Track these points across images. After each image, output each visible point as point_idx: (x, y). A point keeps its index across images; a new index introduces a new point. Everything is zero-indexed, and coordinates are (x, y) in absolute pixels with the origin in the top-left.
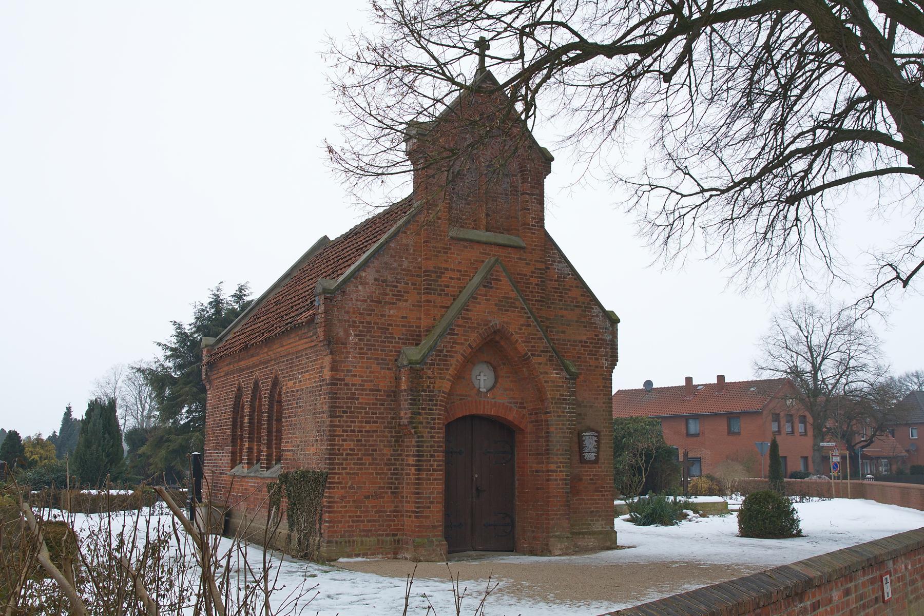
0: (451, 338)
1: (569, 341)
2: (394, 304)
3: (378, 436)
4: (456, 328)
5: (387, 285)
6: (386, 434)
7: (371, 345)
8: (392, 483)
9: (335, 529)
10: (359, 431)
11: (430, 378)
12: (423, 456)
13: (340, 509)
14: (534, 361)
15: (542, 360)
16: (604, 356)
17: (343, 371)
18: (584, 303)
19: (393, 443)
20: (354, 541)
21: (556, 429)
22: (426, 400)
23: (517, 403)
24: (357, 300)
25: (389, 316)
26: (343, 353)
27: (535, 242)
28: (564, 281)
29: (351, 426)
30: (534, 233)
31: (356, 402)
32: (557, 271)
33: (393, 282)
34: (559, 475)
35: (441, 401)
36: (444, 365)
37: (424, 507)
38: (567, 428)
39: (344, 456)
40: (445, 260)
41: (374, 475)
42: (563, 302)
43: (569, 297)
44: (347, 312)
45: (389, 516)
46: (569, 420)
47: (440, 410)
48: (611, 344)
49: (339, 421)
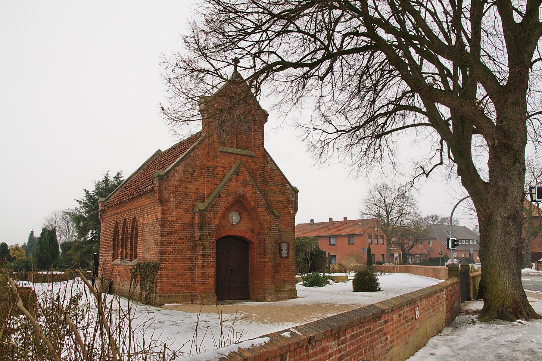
1: (275, 201)
2: (192, 182)
4: (222, 194)
8: (190, 268)
10: (175, 243)
11: (209, 218)
12: (205, 255)
14: (258, 210)
15: (262, 209)
16: (292, 208)
17: (167, 214)
20: (172, 296)
24: (174, 180)
29: (171, 241)
30: (259, 150)
33: (192, 172)
36: (216, 212)
37: (205, 279)
44: (170, 186)
46: (275, 238)
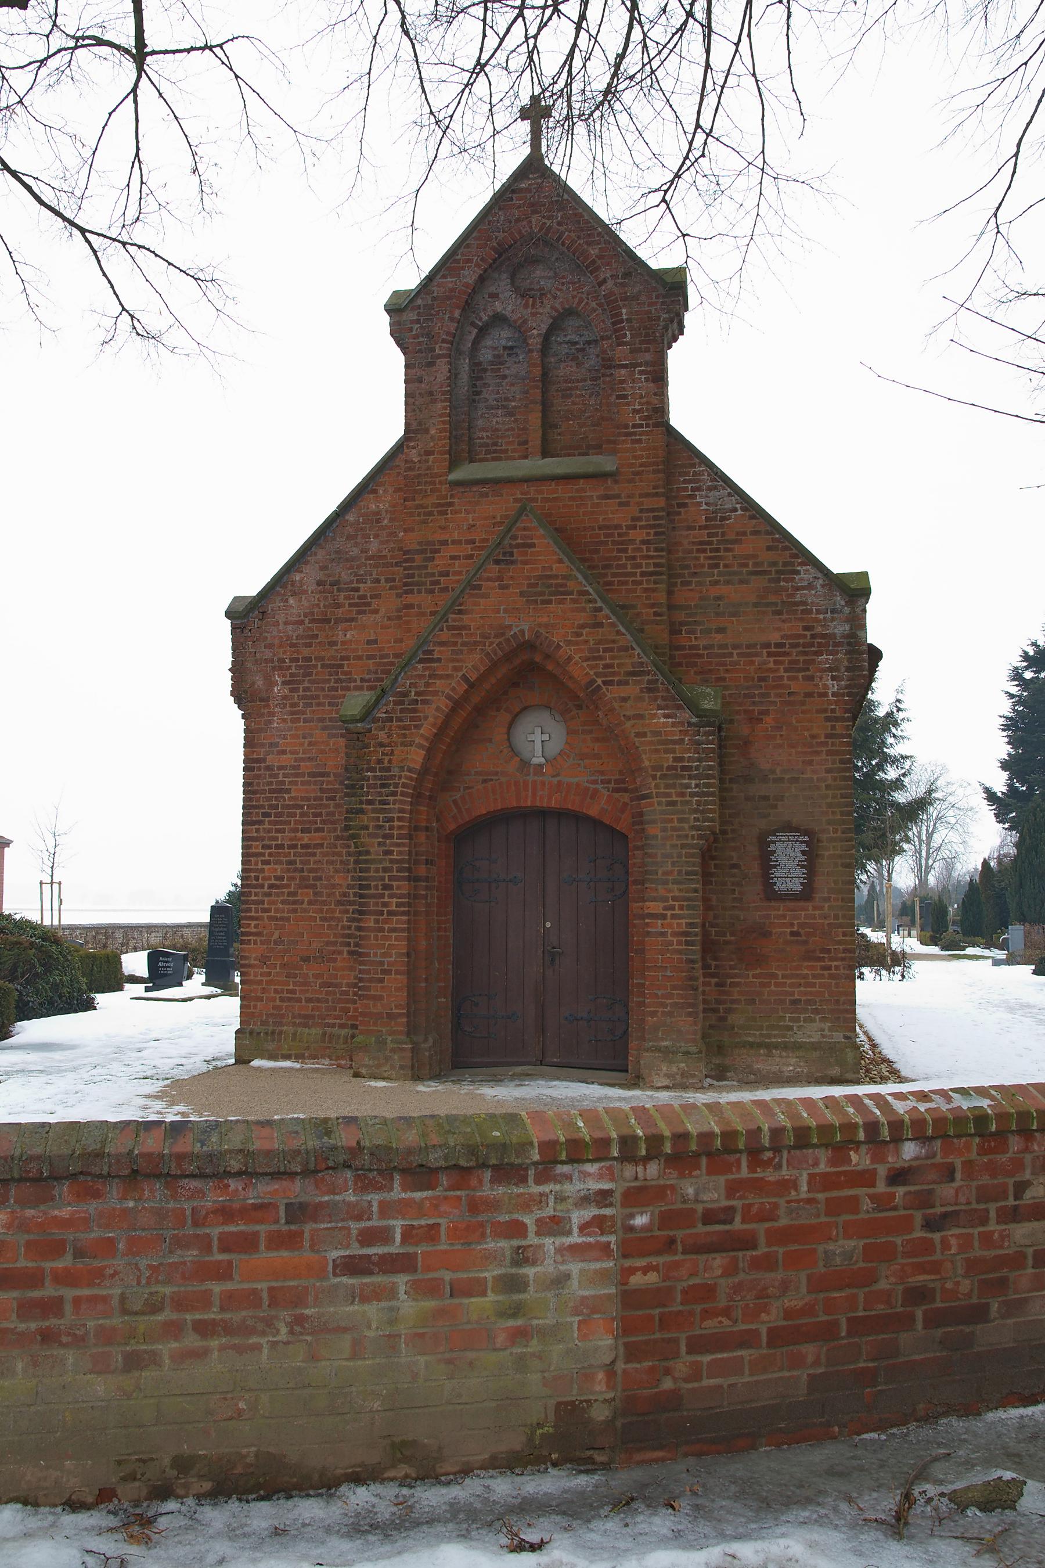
0: (425, 669)
1: (735, 647)
2: (352, 620)
3: (324, 855)
4: (437, 649)
5: (339, 590)
6: (339, 849)
7: (312, 697)
8: (349, 936)
9: (252, 1010)
10: (291, 847)
11: (381, 745)
12: (368, 887)
13: (259, 978)
14: (609, 695)
15: (631, 690)
16: (830, 669)
17: (263, 745)
18: (774, 564)
19: (351, 866)
20: (281, 1033)
21: (664, 830)
22: (375, 786)
23: (609, 782)
24: (286, 623)
25: (343, 643)
26: (263, 715)
27: (642, 457)
28: (722, 526)
29: (276, 839)
30: (639, 441)
31: (286, 796)
32: (704, 507)
33: (352, 582)
34: (670, 926)
35: (404, 785)
36: (412, 719)
37: (370, 980)
38: (693, 828)
39: (266, 889)
40: (440, 527)
41: (318, 922)
42: (721, 569)
43: (734, 557)
44: (270, 646)
45: (347, 993)
46: (696, 811)
47: (402, 802)
48: (849, 644)
49: (257, 831)
